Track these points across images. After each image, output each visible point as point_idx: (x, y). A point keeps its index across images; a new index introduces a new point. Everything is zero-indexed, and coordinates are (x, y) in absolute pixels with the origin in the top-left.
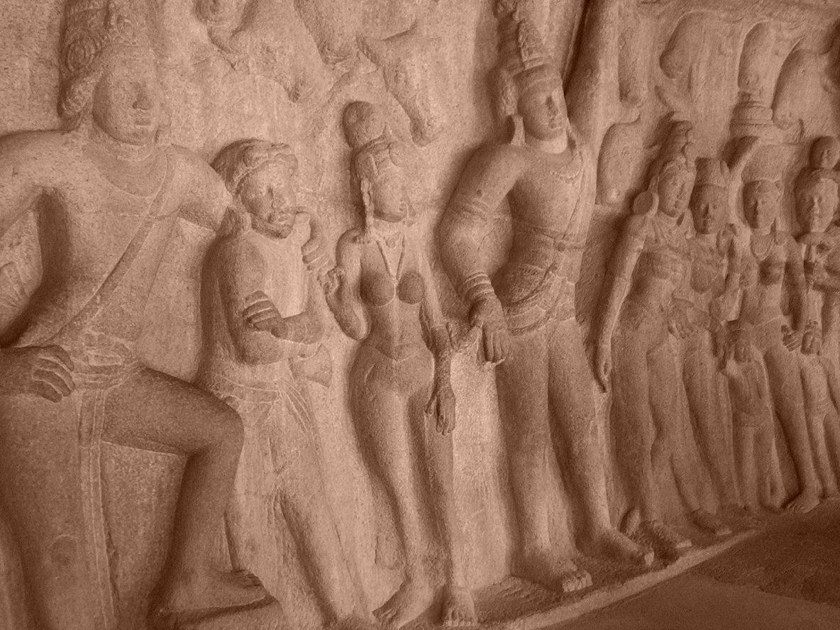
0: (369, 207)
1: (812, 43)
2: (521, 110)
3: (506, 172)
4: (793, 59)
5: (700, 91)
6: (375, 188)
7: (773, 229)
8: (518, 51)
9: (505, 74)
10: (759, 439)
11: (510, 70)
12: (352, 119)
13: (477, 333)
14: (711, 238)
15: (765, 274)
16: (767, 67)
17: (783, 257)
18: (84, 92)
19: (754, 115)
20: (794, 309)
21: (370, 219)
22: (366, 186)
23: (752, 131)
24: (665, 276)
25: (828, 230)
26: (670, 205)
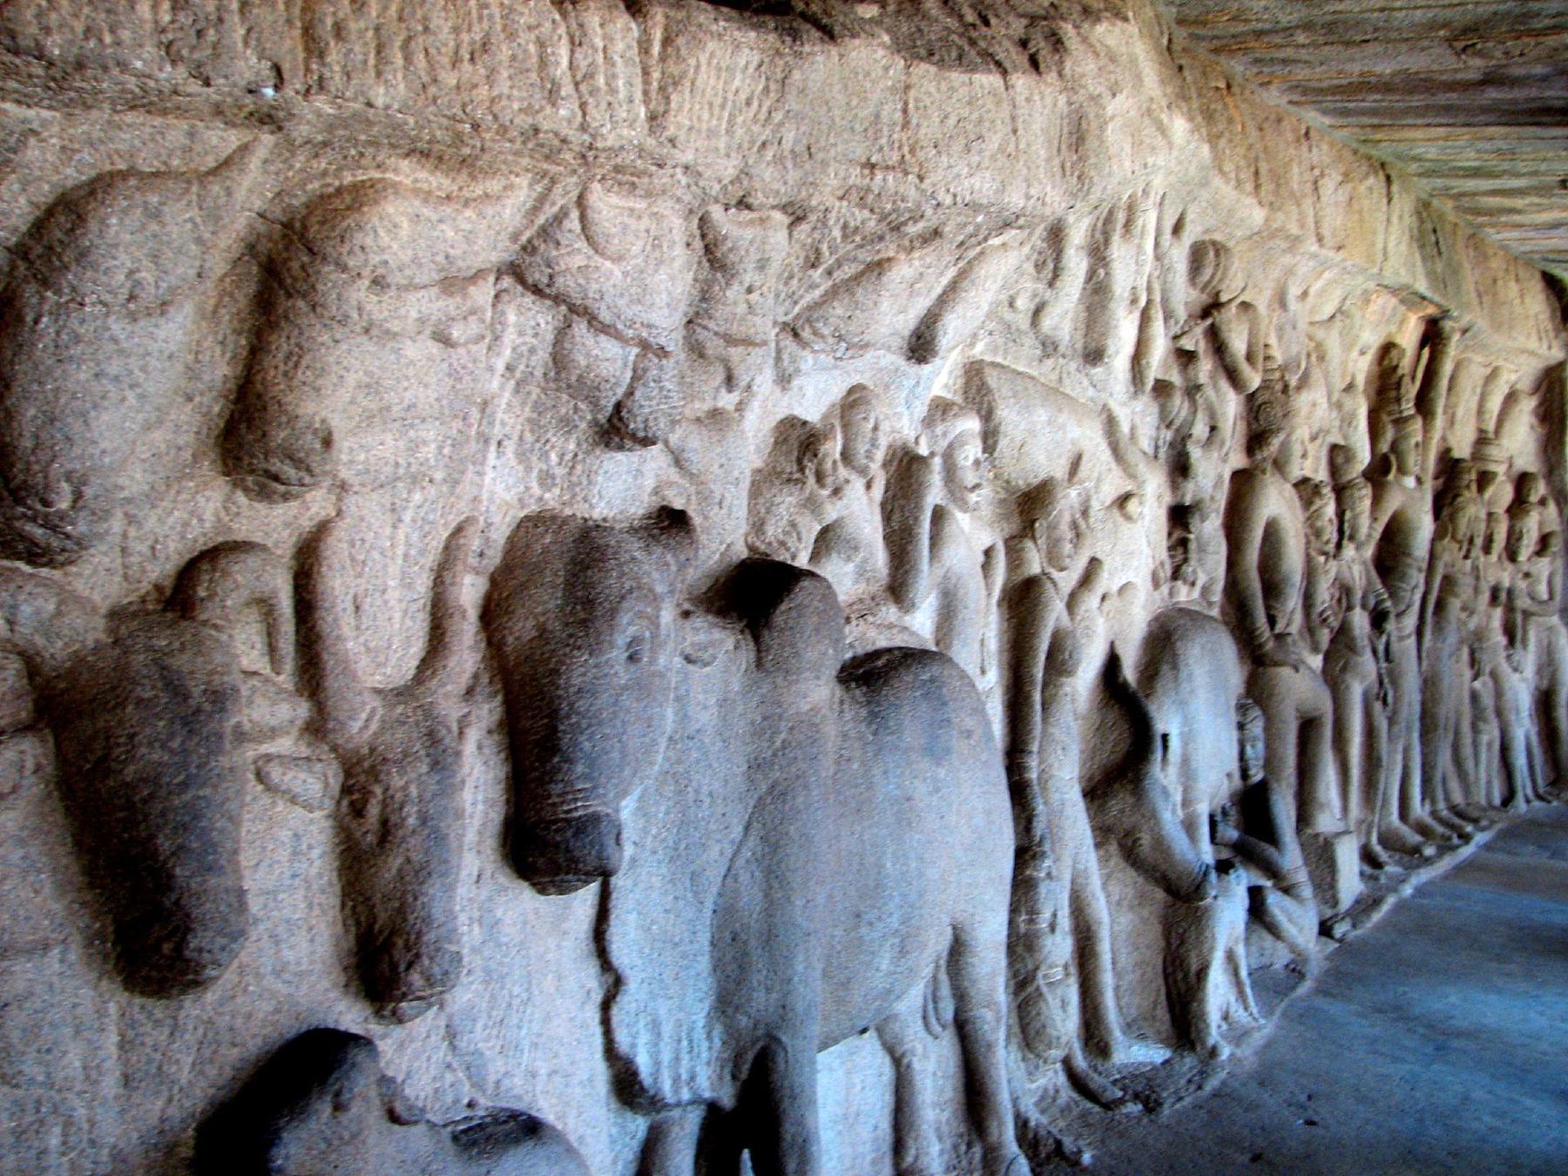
0: (1347, 533)
1: (1525, 384)
2: (1394, 447)
3: (1393, 503)
4: (1511, 398)
5: (1457, 426)
6: (1355, 517)
7: (1500, 558)
8: (1398, 400)
9: (1385, 418)
10: (1490, 745)
11: (1389, 414)
12: (1340, 460)
13: (1384, 638)
14: (1469, 562)
15: (1494, 598)
16: (1495, 404)
17: (1506, 583)
18: (1275, 443)
19: (1493, 451)
20: (1510, 631)
21: (1345, 542)
22: (1348, 515)
23: (1492, 467)
24: (1456, 595)
25: (1529, 559)
26: (1460, 536)
